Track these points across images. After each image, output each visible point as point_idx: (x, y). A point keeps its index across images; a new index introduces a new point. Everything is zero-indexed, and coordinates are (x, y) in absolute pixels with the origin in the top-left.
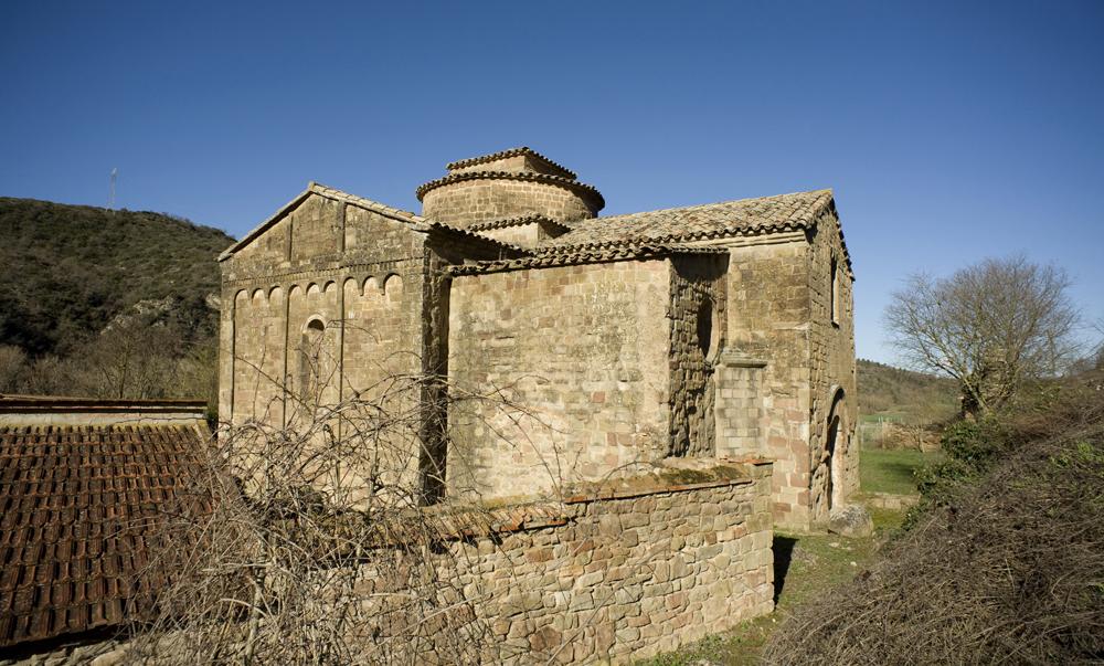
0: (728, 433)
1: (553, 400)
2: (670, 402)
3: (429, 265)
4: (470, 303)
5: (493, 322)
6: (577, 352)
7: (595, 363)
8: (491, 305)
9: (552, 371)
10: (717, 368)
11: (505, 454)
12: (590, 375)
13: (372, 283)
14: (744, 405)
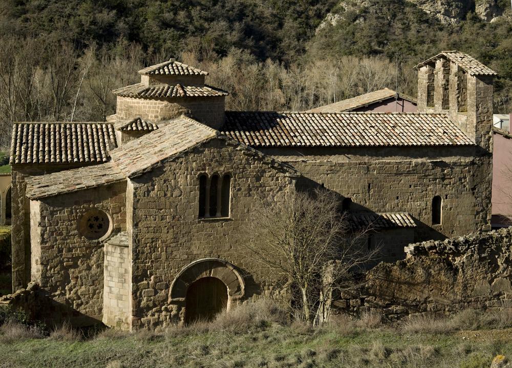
0: (109, 279)
10: (105, 244)
14: (117, 265)
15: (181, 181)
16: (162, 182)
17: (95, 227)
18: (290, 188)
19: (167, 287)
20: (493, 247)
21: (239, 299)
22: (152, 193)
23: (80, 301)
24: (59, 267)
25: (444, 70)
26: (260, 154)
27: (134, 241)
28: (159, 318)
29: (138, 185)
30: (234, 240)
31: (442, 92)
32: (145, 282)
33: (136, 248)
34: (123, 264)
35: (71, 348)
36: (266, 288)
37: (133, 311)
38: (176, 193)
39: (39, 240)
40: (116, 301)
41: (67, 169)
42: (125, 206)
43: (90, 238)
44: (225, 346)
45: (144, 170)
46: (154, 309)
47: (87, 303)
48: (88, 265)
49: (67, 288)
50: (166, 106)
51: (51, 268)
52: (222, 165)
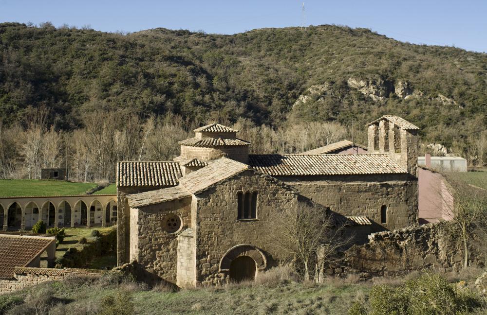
0: (181, 257)
14: (186, 249)
15: (226, 196)
16: (215, 197)
17: (172, 225)
18: (294, 200)
19: (218, 262)
20: (425, 235)
21: (263, 270)
22: (209, 204)
23: (162, 271)
24: (149, 250)
25: (385, 127)
26: (276, 179)
27: (198, 233)
28: (213, 282)
29: (199, 199)
30: (259, 233)
31: (384, 141)
32: (204, 259)
33: (199, 237)
35: (167, 296)
36: (280, 262)
37: (197, 277)
38: (224, 203)
39: (137, 233)
40: (186, 270)
41: (152, 190)
42: (190, 212)
43: (169, 232)
44: (264, 295)
45: (204, 189)
46: (210, 276)
47: (167, 272)
48: (167, 248)
49: (154, 263)
50: (213, 151)
51: (144, 251)
52: (252, 186)
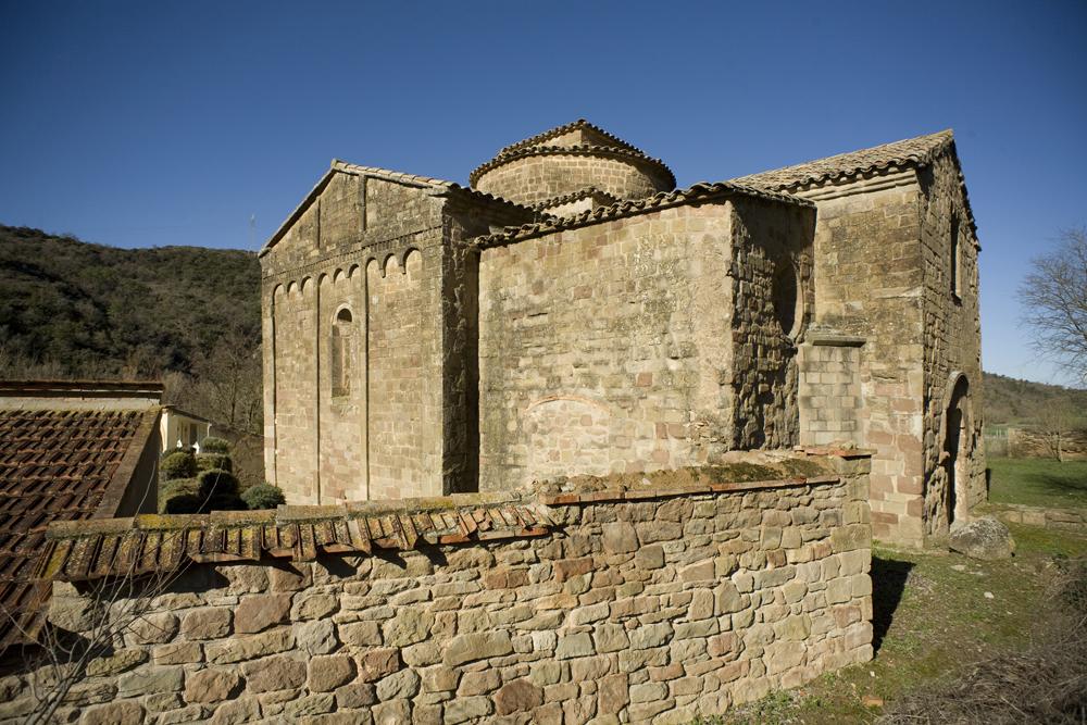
0: (815, 426)
1: (592, 386)
2: (734, 384)
3: (450, 235)
4: (499, 279)
5: (524, 298)
6: (618, 326)
7: (639, 338)
8: (522, 279)
9: (590, 351)
10: (800, 347)
11: (539, 451)
12: (634, 352)
13: (393, 262)
14: (836, 390)
34: (849, 387)
